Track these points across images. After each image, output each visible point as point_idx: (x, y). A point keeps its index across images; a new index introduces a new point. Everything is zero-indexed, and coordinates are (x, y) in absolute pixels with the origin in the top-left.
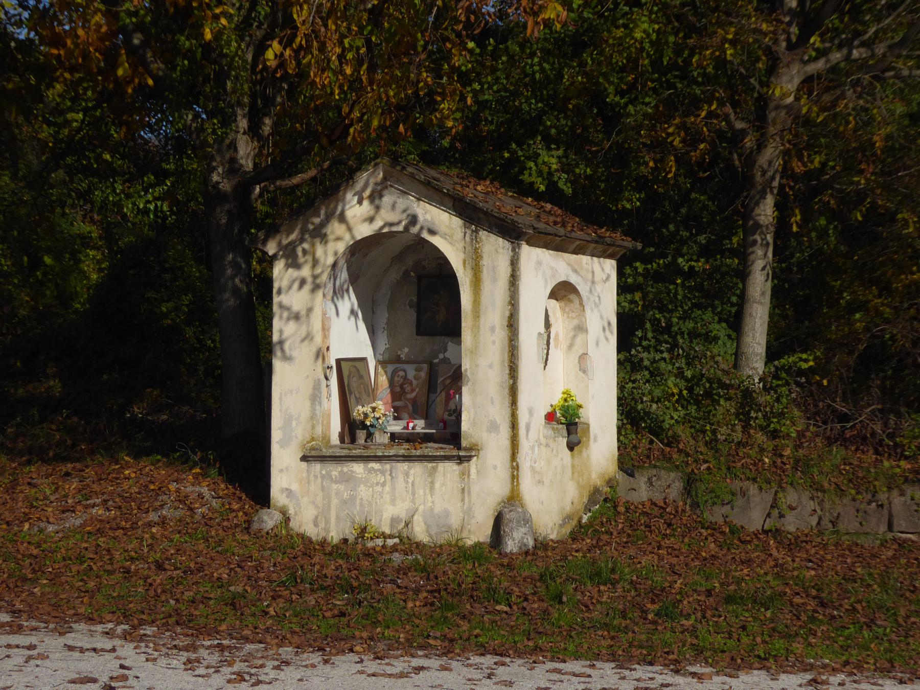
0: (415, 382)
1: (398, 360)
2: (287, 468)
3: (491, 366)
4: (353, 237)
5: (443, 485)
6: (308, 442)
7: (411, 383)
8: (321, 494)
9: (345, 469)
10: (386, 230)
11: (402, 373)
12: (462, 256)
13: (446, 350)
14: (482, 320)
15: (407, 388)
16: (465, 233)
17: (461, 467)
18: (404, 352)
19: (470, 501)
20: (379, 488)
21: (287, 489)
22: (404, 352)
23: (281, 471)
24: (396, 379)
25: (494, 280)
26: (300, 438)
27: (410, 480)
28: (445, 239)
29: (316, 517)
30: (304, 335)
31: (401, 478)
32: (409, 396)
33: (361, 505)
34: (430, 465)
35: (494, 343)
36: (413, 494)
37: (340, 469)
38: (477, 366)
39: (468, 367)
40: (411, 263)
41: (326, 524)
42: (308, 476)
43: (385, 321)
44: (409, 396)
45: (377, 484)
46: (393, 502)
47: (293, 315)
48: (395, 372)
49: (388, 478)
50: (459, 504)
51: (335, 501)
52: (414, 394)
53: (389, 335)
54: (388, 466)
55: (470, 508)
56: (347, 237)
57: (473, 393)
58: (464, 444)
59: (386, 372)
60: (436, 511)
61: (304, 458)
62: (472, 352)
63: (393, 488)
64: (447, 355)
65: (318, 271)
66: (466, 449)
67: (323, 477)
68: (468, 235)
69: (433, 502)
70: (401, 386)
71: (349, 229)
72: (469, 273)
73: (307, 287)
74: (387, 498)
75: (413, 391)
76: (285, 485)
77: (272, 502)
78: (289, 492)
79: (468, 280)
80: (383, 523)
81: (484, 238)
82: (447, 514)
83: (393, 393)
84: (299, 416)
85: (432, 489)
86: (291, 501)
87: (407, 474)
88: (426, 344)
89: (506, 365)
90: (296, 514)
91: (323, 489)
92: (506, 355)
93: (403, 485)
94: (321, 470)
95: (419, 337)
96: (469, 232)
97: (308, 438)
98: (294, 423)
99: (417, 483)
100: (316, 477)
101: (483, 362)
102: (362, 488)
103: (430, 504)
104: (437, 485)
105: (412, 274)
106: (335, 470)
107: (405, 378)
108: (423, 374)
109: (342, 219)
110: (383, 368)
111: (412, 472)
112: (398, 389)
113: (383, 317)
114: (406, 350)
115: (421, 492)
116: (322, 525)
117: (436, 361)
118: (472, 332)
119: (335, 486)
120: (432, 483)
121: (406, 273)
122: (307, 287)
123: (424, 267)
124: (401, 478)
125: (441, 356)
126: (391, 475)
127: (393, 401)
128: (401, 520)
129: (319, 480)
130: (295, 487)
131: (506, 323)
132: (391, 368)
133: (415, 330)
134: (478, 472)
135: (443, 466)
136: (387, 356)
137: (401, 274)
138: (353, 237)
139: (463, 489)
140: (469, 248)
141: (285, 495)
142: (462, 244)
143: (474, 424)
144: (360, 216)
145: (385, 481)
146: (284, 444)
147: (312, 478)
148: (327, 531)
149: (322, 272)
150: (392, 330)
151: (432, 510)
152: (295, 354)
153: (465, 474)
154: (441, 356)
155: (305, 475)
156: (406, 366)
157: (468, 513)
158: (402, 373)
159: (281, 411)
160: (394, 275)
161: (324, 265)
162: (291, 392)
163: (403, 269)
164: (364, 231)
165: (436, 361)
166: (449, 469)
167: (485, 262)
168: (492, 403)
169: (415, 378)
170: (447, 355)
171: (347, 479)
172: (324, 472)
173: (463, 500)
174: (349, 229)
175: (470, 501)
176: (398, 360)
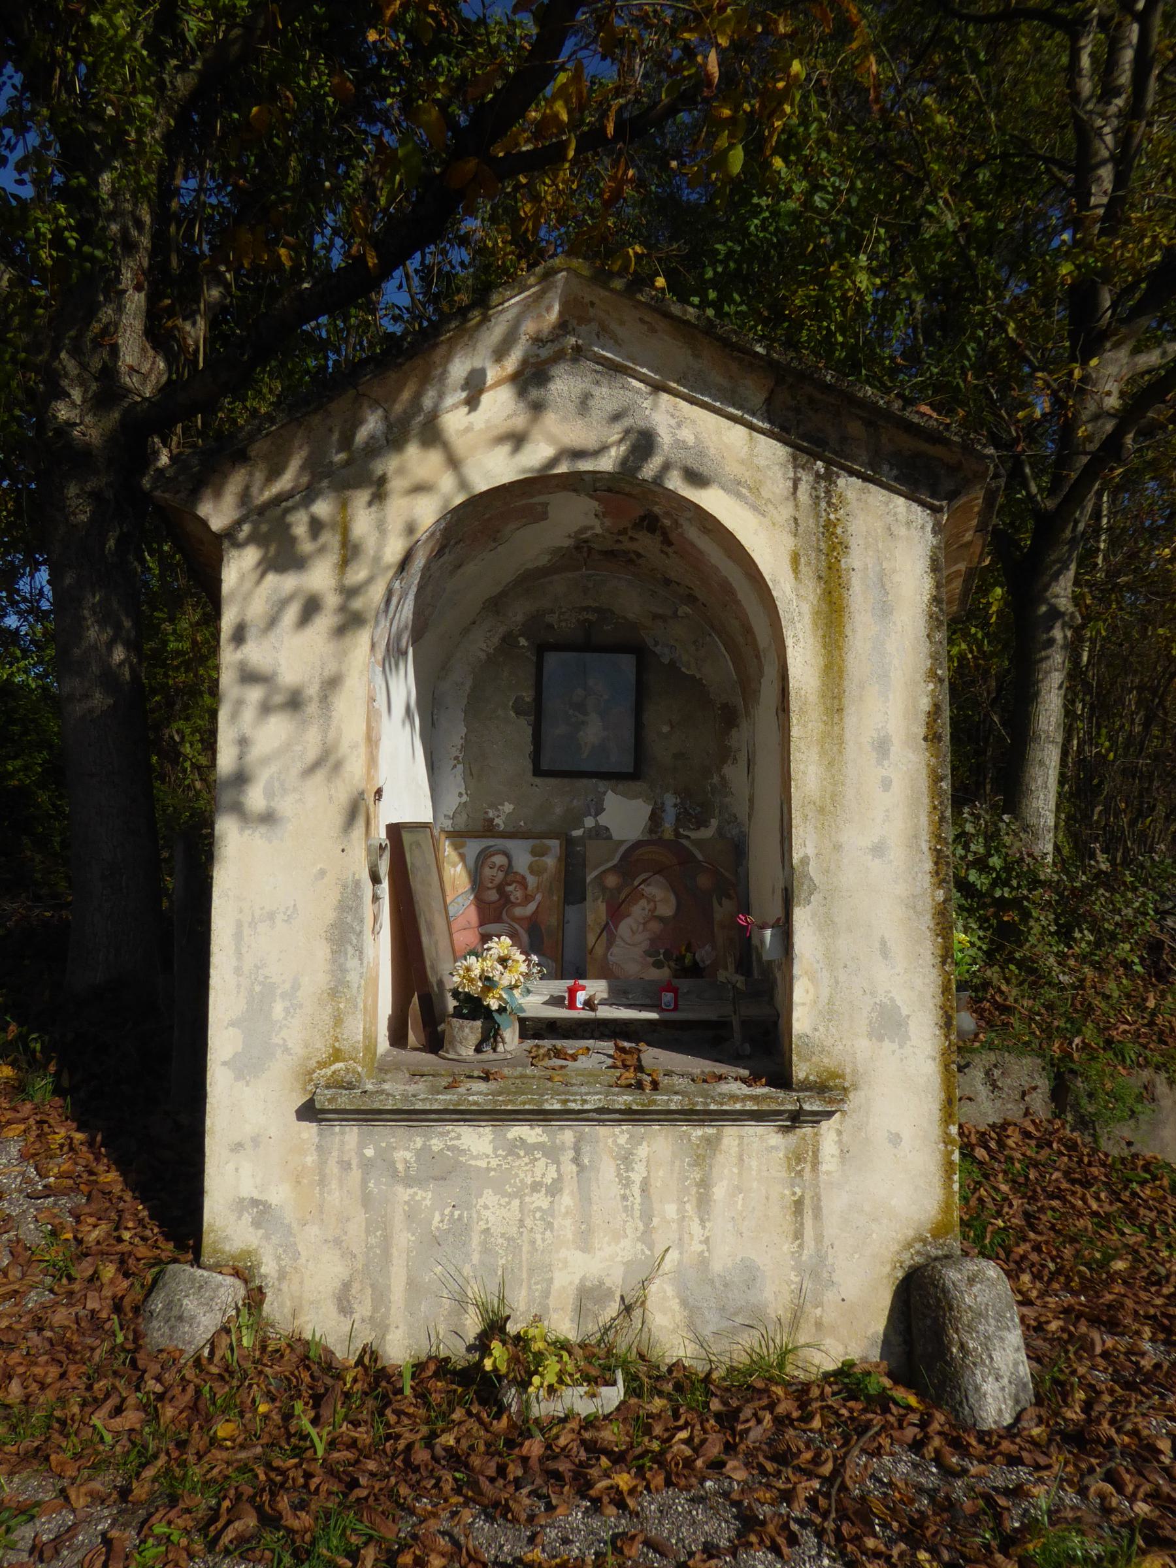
0: (532, 881)
1: (488, 830)
2: (256, 1141)
3: (878, 850)
4: (463, 484)
5: (739, 1189)
6: (322, 1065)
7: (523, 883)
8: (359, 1218)
9: (436, 1144)
10: (563, 468)
11: (499, 860)
12: (788, 543)
13: (600, 810)
15: (516, 893)
16: (796, 482)
17: (793, 1138)
18: (503, 813)
19: (819, 1238)
20: (540, 1200)
21: (255, 1202)
22: (503, 813)
23: (238, 1147)
24: (487, 872)
25: (884, 611)
26: (299, 1050)
27: (636, 1177)
28: (739, 495)
29: (346, 1286)
30: (312, 755)
31: (608, 1169)
32: (518, 911)
33: (486, 1249)
34: (698, 1132)
35: (886, 784)
36: (647, 1216)
37: (419, 1142)
38: (838, 847)
39: (810, 851)
40: (520, 618)
41: (375, 1309)
42: (322, 1163)
43: (459, 742)
44: (518, 911)
45: (535, 1187)
46: (584, 1241)
47: (278, 699)
48: (483, 857)
49: (570, 1169)
50: (787, 1247)
51: (403, 1239)
52: (531, 907)
53: (469, 775)
54: (567, 1135)
55: (821, 1257)
56: (447, 482)
57: (827, 925)
58: (801, 1071)
59: (462, 857)
60: (717, 1266)
61: (309, 1112)
62: (822, 810)
63: (585, 1199)
64: (603, 820)
65: (358, 574)
66: (806, 1086)
67: (367, 1166)
68: (803, 487)
69: (707, 1241)
70: (500, 889)
71: (453, 462)
72: (811, 590)
73: (324, 622)
74: (567, 1227)
75: (528, 899)
76: (248, 1189)
77: (208, 1239)
78: (260, 1211)
79: (806, 608)
80: (552, 1302)
81: (851, 495)
82: (750, 1275)
83: (481, 904)
84: (296, 986)
85: (704, 1201)
86: (267, 1237)
87: (626, 1159)
88: (557, 798)
89: (925, 847)
90: (282, 1275)
91: (366, 1200)
92: (924, 820)
93: (616, 1190)
94: (362, 1145)
95: (538, 781)
96: (806, 479)
97: (322, 1050)
98: (278, 1009)
99: (656, 1184)
100: (345, 1166)
101: (856, 838)
102: (489, 1197)
103: (697, 1247)
104: (719, 1192)
105: (523, 642)
106: (406, 1146)
107: (509, 869)
108: (550, 862)
109: (432, 435)
110: (456, 847)
111: (642, 1151)
112: (493, 896)
113: (455, 734)
114: (508, 808)
115: (671, 1210)
116: (363, 1309)
117: (577, 833)
118: (823, 753)
119: (403, 1194)
120: (705, 1184)
121: (508, 640)
122: (324, 622)
123: (550, 626)
124: (608, 1169)
125: (589, 822)
126: (576, 1160)
127: (481, 924)
128: (609, 1293)
129: (356, 1174)
130: (279, 1195)
131: (921, 731)
132: (474, 847)
133: (529, 766)
134: (844, 1153)
135: (731, 1135)
136: (462, 820)
137: (496, 640)
138: (463, 484)
139: (799, 1204)
140: (808, 523)
141: (247, 1218)
142: (786, 512)
143: (829, 1013)
144: (485, 431)
145: (559, 1180)
146: (246, 1067)
147: (333, 1168)
148: (382, 1328)
149: (370, 580)
150: (475, 763)
151: (703, 1263)
152: (286, 806)
153: (803, 1161)
154: (589, 822)
155: (311, 1159)
156: (510, 844)
157: (816, 1272)
158: (499, 860)
159: (238, 971)
160: (481, 643)
161: (377, 559)
162: (271, 916)
163: (502, 630)
164: (495, 469)
165: (577, 833)
167: (858, 560)
168: (885, 951)
169: (532, 870)
170: (603, 820)
171: (443, 1171)
172: (369, 1152)
173: (798, 1235)
174: (453, 462)
175: (819, 1238)
176: (488, 830)
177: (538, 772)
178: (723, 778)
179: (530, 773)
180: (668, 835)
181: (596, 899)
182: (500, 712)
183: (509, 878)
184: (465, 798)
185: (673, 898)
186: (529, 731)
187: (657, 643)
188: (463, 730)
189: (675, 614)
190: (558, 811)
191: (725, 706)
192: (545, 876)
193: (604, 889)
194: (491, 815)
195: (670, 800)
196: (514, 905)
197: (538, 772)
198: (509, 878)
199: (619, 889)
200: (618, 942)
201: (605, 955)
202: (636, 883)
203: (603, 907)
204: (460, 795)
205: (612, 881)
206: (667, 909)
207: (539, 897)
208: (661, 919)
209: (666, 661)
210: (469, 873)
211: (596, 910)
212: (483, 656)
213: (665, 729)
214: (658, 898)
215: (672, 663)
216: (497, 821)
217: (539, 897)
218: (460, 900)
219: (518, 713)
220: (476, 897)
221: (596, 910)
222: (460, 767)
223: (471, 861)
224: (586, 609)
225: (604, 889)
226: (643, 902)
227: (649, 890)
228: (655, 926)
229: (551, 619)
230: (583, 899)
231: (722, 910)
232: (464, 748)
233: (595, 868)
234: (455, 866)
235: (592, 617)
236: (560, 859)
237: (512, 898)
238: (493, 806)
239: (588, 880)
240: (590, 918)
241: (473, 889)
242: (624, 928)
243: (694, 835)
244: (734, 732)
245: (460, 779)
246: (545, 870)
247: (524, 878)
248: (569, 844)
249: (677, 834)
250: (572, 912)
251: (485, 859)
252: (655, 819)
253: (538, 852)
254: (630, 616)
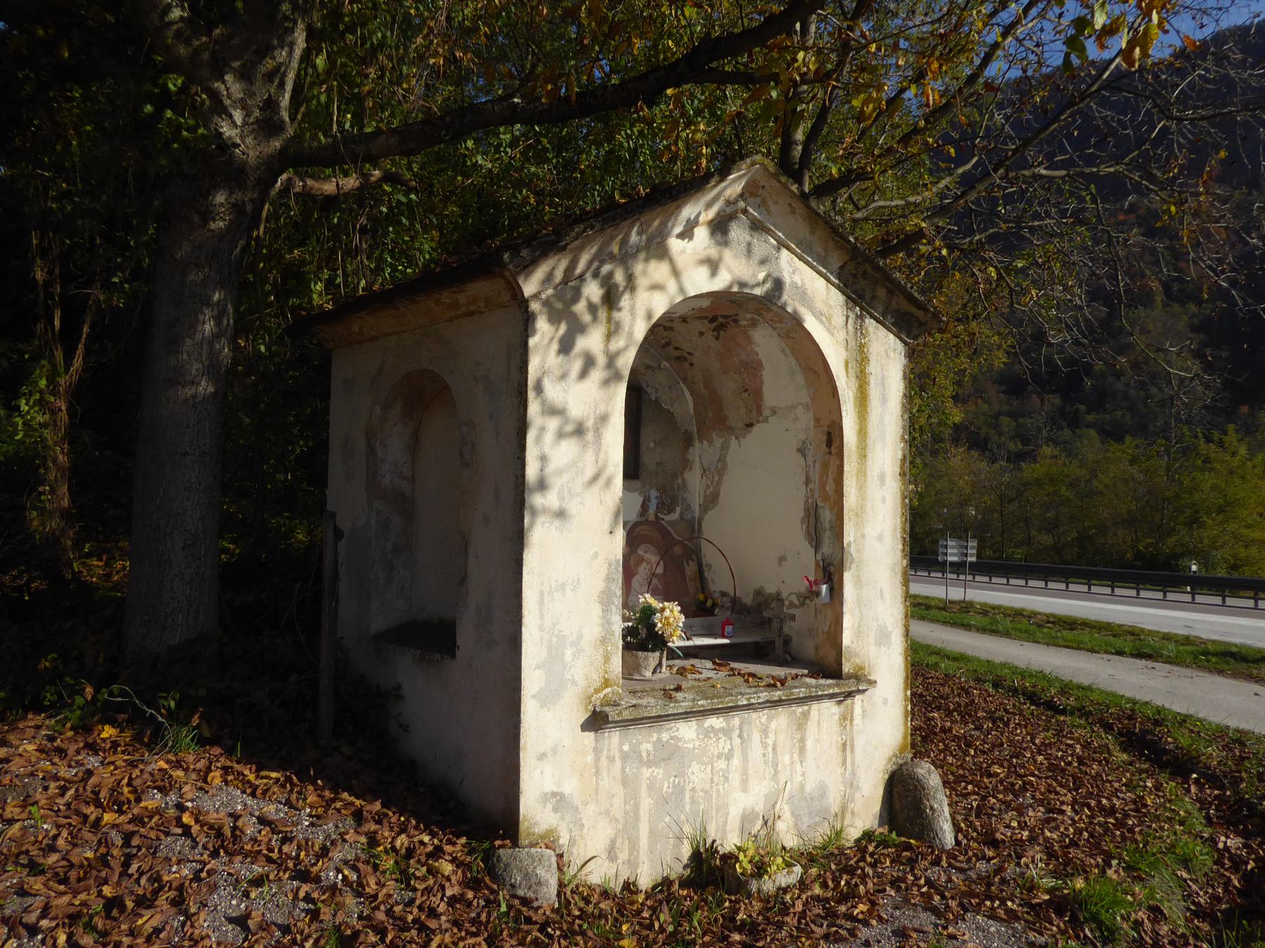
2: (554, 751)
3: (880, 538)
4: (682, 290)
5: (818, 741)
6: (597, 691)
8: (620, 792)
9: (665, 736)
10: (735, 289)
12: (843, 354)
14: (869, 462)
16: (847, 317)
17: (842, 707)
19: (853, 764)
20: (721, 764)
21: (554, 794)
23: (542, 757)
25: (884, 400)
26: (582, 682)
27: (770, 742)
28: (822, 322)
29: (613, 842)
30: (589, 473)
31: (756, 737)
33: (693, 801)
34: (800, 710)
35: (884, 500)
36: (775, 765)
37: (655, 736)
38: (863, 536)
39: (852, 539)
41: (631, 854)
42: (597, 759)
45: (719, 756)
46: (744, 786)
47: (569, 428)
49: (737, 741)
50: (840, 771)
51: (646, 803)
54: (736, 721)
55: (854, 774)
56: (672, 286)
57: (858, 581)
58: (847, 668)
60: (808, 789)
62: (857, 515)
63: (745, 759)
65: (618, 343)
66: (849, 677)
67: (625, 757)
68: (851, 321)
69: (803, 775)
71: (676, 273)
72: (854, 384)
73: (597, 375)
74: (735, 779)
76: (549, 786)
77: (523, 827)
78: (558, 800)
79: (851, 395)
80: (728, 828)
81: (871, 330)
82: (823, 790)
84: (580, 636)
85: (802, 751)
86: (563, 818)
87: (765, 732)
89: (899, 536)
90: (572, 841)
91: (625, 782)
92: (899, 520)
93: (760, 751)
94: (621, 744)
96: (852, 316)
97: (597, 680)
98: (568, 654)
99: (780, 744)
100: (611, 759)
101: (871, 530)
102: (695, 767)
103: (799, 779)
104: (809, 744)
106: (646, 740)
109: (662, 253)
111: (773, 725)
115: (787, 759)
116: (623, 856)
118: (858, 481)
119: (646, 773)
120: (802, 741)
122: (597, 375)
124: (756, 737)
126: (740, 736)
128: (758, 814)
129: (618, 763)
130: (570, 787)
131: (898, 470)
134: (864, 712)
135: (815, 707)
138: (682, 290)
139: (844, 745)
140: (852, 343)
141: (549, 806)
142: (842, 335)
143: (858, 633)
145: (731, 750)
146: (547, 699)
147: (604, 761)
148: (633, 863)
149: (626, 348)
151: (802, 787)
152: (573, 507)
153: (846, 718)
155: (590, 758)
157: (852, 784)
159: (541, 628)
161: (631, 334)
162: (563, 587)
164: (700, 282)
166: (825, 712)
167: (873, 368)
168: (882, 595)
171: (670, 754)
172: (626, 748)
173: (844, 763)
174: (676, 273)
175: (853, 764)
178: (684, 480)
180: (652, 518)
191: (686, 432)
195: (654, 494)
213: (652, 445)
231: (690, 569)
243: (667, 518)
244: (691, 450)
249: (656, 515)
252: (644, 506)
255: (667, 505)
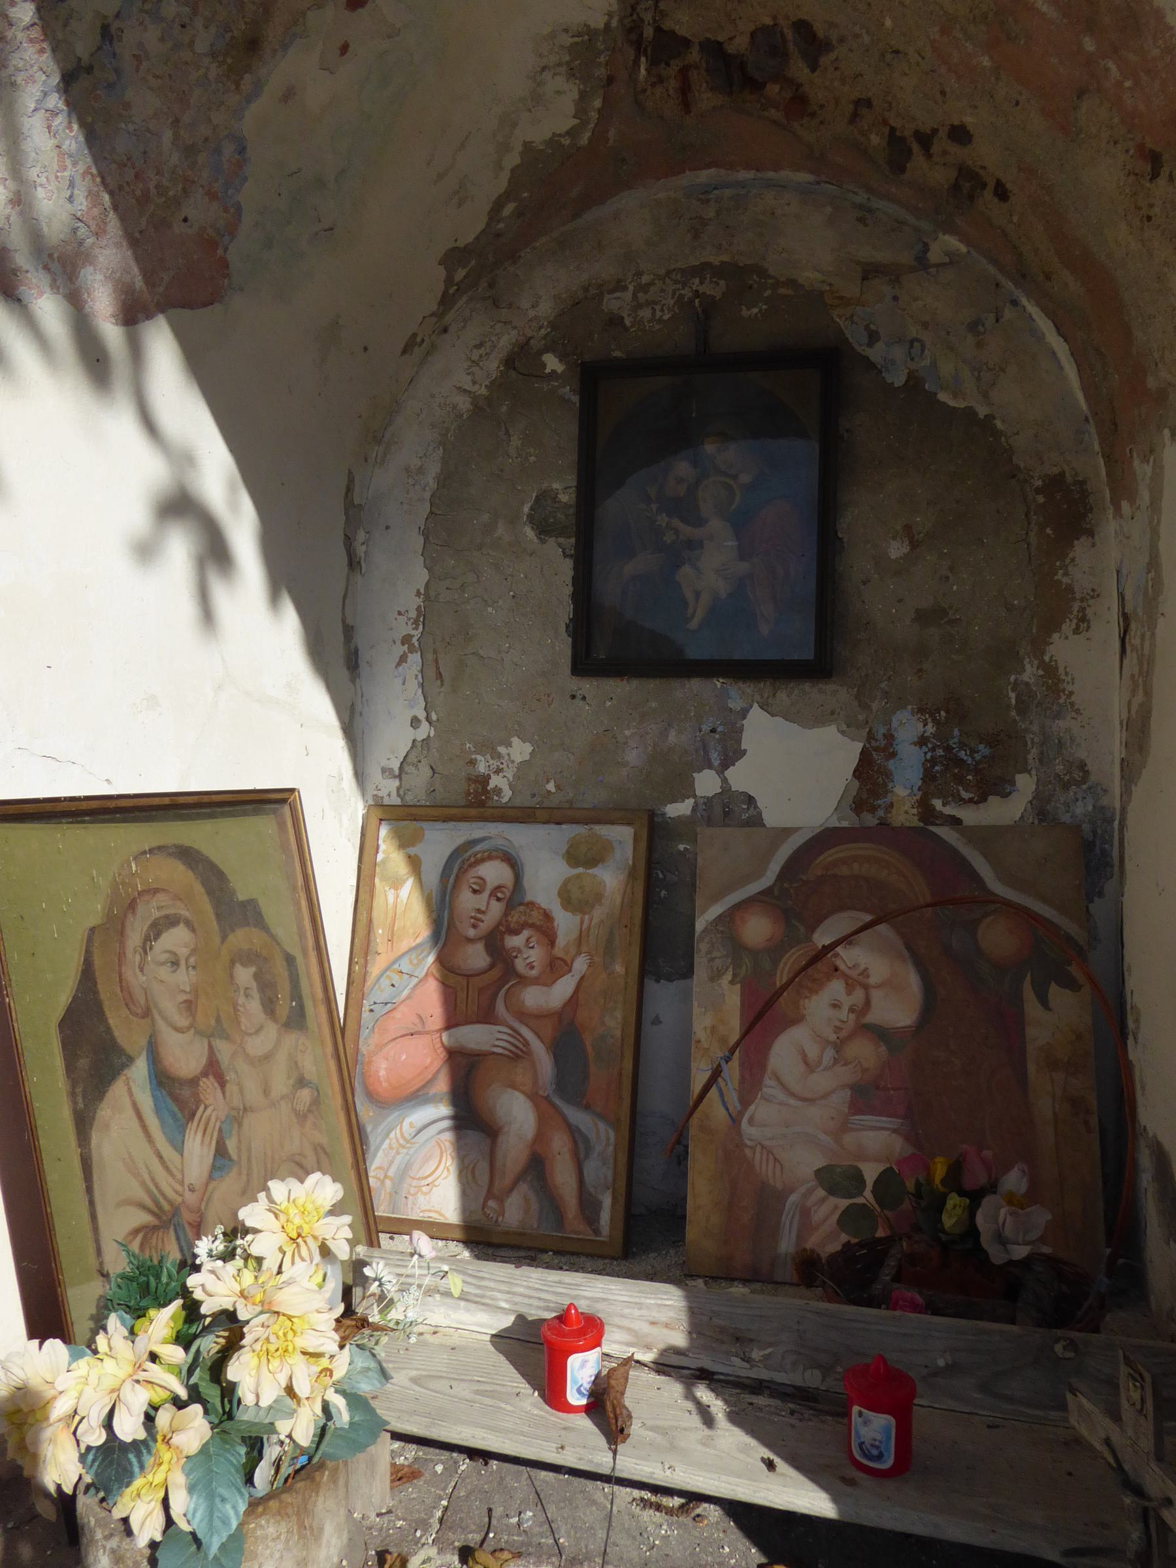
0: (565, 923)
1: (477, 803)
7: (546, 931)
11: (494, 873)
13: (732, 755)
15: (528, 953)
18: (510, 764)
22: (510, 764)
24: (467, 901)
32: (533, 998)
40: (546, 309)
43: (412, 603)
44: (533, 998)
48: (459, 865)
52: (563, 988)
53: (434, 677)
59: (415, 864)
64: (740, 777)
70: (493, 942)
75: (556, 967)
83: (450, 972)
88: (625, 721)
95: (587, 686)
105: (552, 363)
107: (514, 897)
108: (611, 879)
110: (404, 842)
112: (476, 957)
113: (400, 583)
114: (520, 750)
117: (679, 809)
121: (522, 361)
123: (615, 321)
125: (707, 783)
127: (450, 1024)
132: (440, 842)
133: (564, 647)
136: (420, 778)
137: (493, 365)
150: (444, 646)
154: (707, 783)
156: (518, 836)
158: (494, 873)
160: (459, 374)
163: (506, 341)
165: (679, 809)
169: (567, 899)
170: (740, 777)
176: (477, 803)
177: (585, 663)
178: (1050, 671)
179: (567, 669)
180: (905, 814)
181: (716, 976)
182: (501, 530)
183: (515, 918)
184: (424, 730)
185: (913, 980)
186: (567, 568)
187: (873, 337)
188: (423, 576)
189: (922, 261)
190: (633, 756)
191: (1055, 483)
192: (598, 913)
193: (737, 948)
194: (482, 768)
195: (908, 728)
196: (523, 981)
197: (585, 663)
198: (515, 918)
199: (776, 950)
200: (769, 1087)
201: (735, 1121)
202: (822, 938)
203: (733, 998)
204: (415, 723)
205: (758, 929)
206: (898, 1010)
207: (580, 965)
208: (880, 1033)
209: (898, 379)
210: (428, 901)
211: (712, 1006)
212: (463, 404)
213: (897, 550)
214: (877, 981)
215: (914, 382)
216: (495, 781)
217: (580, 965)
218: (405, 965)
219: (544, 529)
220: (441, 960)
221: (712, 1006)
222: (415, 659)
223: (433, 876)
224: (700, 270)
225: (737, 948)
226: (836, 987)
227: (850, 957)
228: (866, 1052)
229: (612, 303)
230: (688, 972)
231: (1054, 1019)
232: (423, 617)
233: (715, 898)
234: (396, 885)
235: (714, 289)
236: (632, 874)
237: (520, 965)
238: (489, 748)
239: (700, 925)
240: (701, 1024)
241: (436, 936)
242: (785, 1052)
243: (970, 816)
244: (1080, 549)
245: (413, 686)
246: (598, 898)
247: (547, 916)
248: (657, 835)
249: (928, 814)
250: (662, 995)
251: (463, 871)
252: (870, 774)
253: (582, 856)
254: (808, 276)
255: (975, 757)
